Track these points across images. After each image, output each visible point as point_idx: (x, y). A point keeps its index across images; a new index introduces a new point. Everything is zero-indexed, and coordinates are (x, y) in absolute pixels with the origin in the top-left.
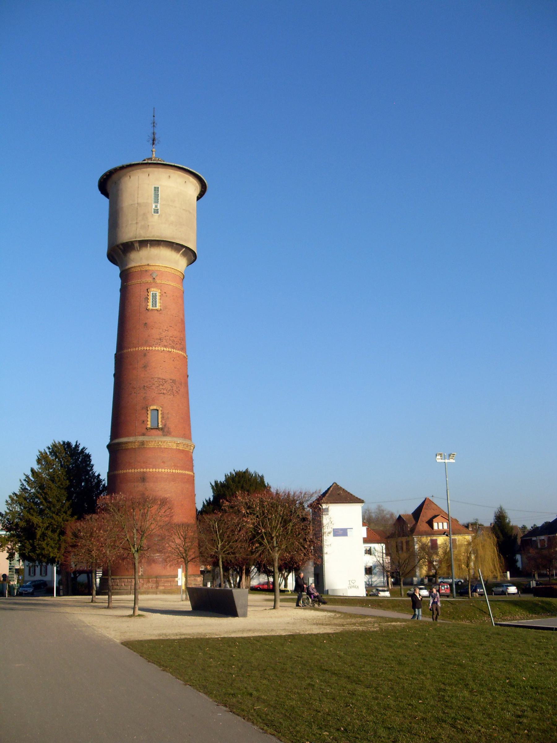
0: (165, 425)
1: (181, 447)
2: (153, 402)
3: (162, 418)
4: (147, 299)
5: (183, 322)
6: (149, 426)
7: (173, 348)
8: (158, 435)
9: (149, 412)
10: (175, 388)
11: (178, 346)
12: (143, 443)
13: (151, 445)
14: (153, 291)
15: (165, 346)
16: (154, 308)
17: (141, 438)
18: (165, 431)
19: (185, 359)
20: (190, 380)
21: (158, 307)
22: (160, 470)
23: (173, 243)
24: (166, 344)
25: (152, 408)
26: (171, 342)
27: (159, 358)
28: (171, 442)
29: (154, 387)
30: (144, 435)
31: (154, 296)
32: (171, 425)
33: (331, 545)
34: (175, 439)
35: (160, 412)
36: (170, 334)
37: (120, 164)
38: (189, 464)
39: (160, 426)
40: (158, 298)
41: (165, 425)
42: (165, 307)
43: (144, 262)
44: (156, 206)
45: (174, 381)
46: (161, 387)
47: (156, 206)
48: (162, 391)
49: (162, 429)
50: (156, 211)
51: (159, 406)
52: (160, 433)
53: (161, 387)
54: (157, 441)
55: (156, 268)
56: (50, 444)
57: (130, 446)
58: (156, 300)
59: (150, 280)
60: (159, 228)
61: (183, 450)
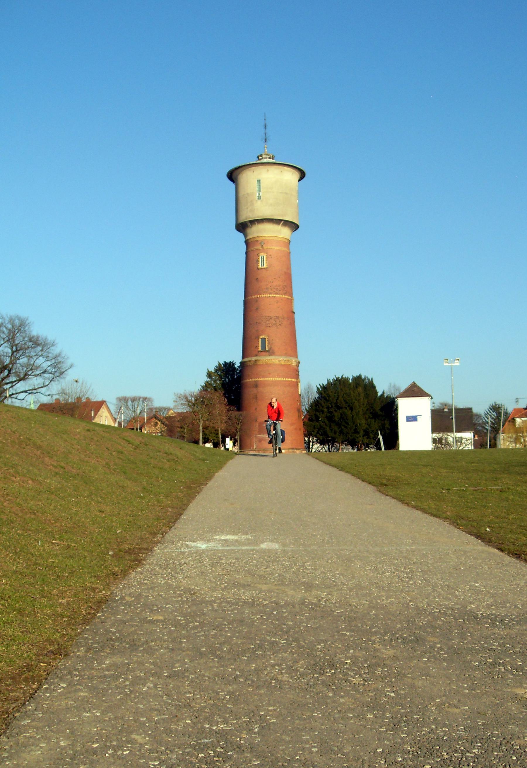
0: (271, 348)
1: (283, 363)
2: (263, 333)
3: (269, 343)
4: (258, 261)
5: (288, 276)
6: (260, 350)
7: (277, 294)
8: (265, 355)
9: (260, 340)
10: (278, 322)
11: (281, 292)
12: (255, 361)
13: (261, 363)
14: (262, 255)
15: (271, 293)
16: (263, 267)
17: (254, 358)
18: (271, 352)
19: (290, 302)
20: (296, 316)
21: (265, 266)
22: (267, 379)
23: (273, 219)
24: (271, 292)
25: (261, 337)
26: (275, 290)
27: (270, 301)
28: (275, 360)
29: (262, 322)
30: (257, 356)
31: (263, 259)
32: (276, 349)
33: (403, 426)
34: (277, 357)
35: (266, 340)
36: (275, 284)
37: (237, 165)
38: (296, 374)
39: (267, 349)
40: (265, 259)
41: (271, 348)
42: (270, 265)
43: (255, 235)
44: (259, 194)
45: (277, 317)
46: (268, 322)
47: (259, 194)
48: (269, 325)
49: (268, 351)
50: (259, 198)
51: (273, 335)
52: (267, 353)
53: (268, 322)
54: (264, 359)
55: (264, 238)
56: (356, 374)
57: (249, 364)
58: (263, 262)
59: (259, 247)
60: (261, 209)
61: (285, 365)
